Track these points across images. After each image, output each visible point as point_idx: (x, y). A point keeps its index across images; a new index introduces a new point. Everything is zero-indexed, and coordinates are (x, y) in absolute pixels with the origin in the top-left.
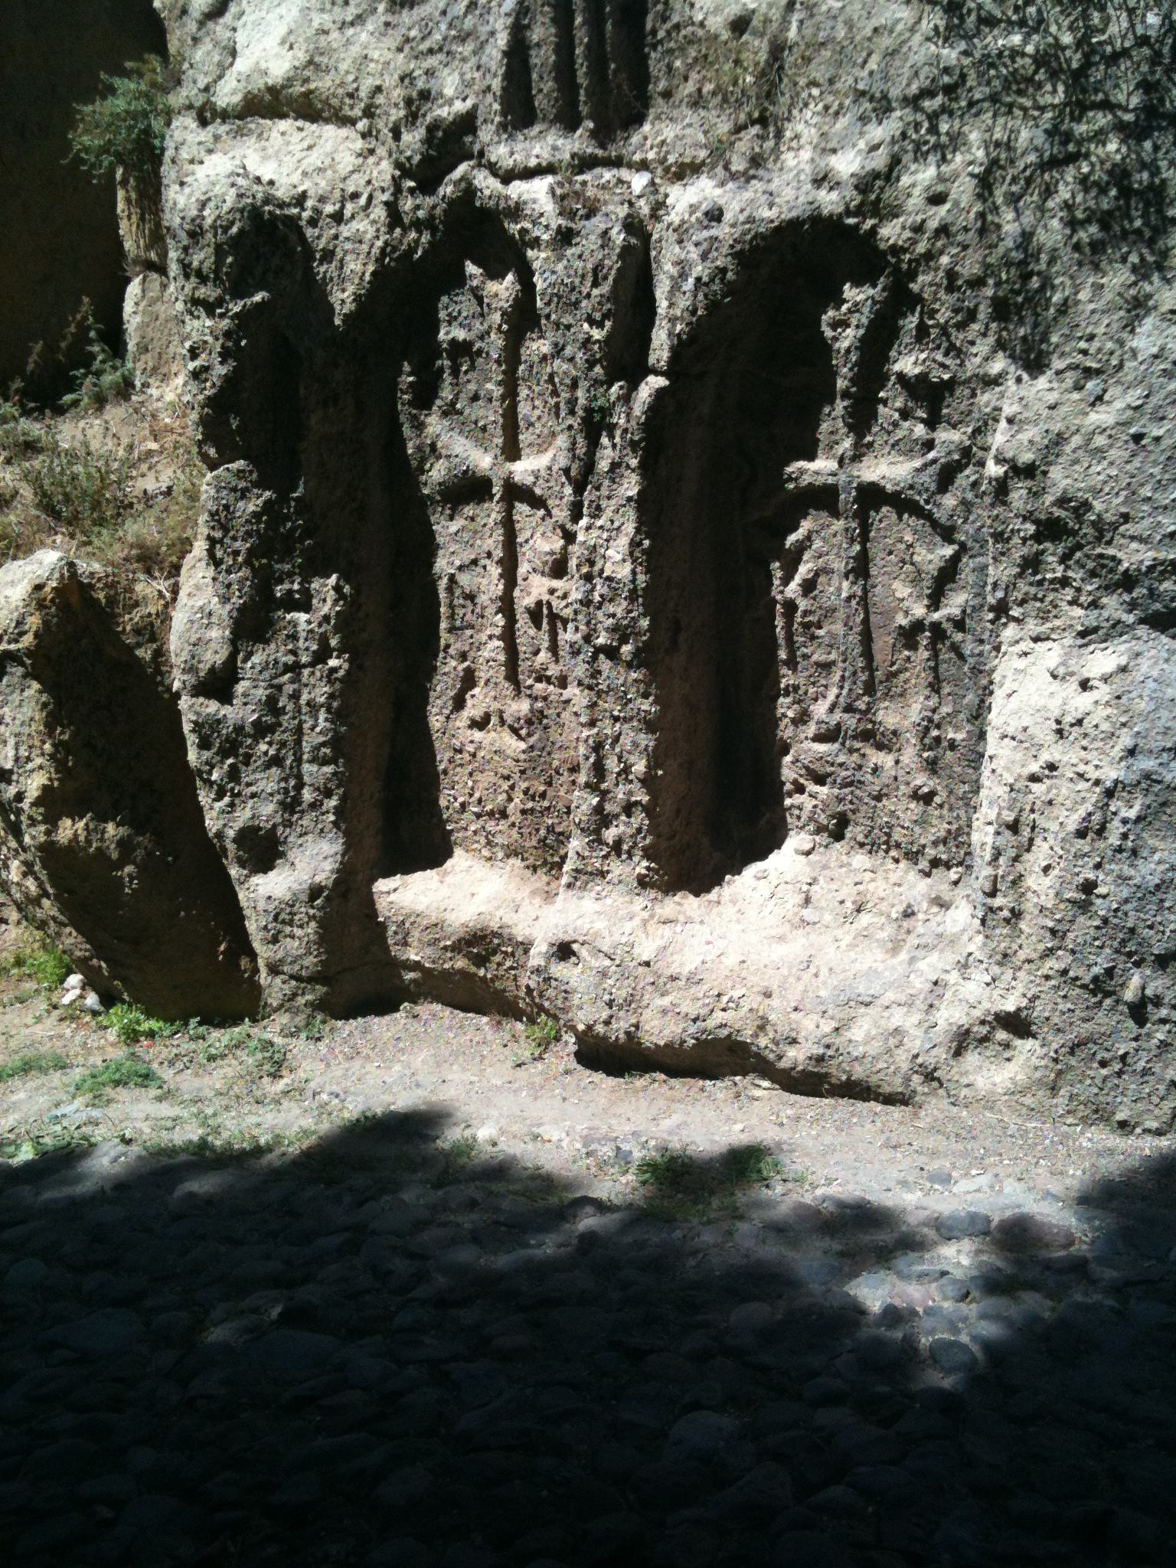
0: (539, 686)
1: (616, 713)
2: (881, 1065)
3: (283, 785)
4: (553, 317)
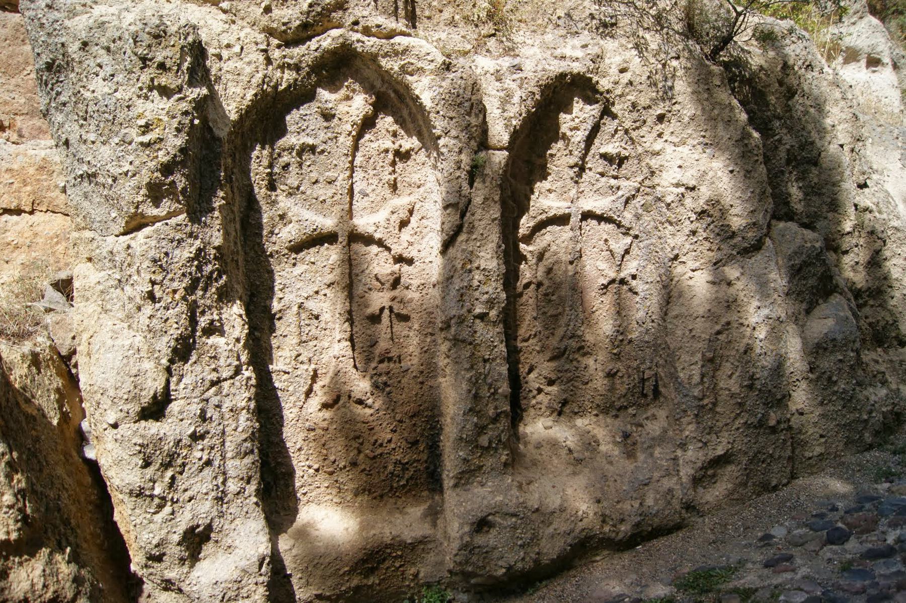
0: (381, 366)
1: (487, 357)
2: (666, 512)
4: (441, 113)
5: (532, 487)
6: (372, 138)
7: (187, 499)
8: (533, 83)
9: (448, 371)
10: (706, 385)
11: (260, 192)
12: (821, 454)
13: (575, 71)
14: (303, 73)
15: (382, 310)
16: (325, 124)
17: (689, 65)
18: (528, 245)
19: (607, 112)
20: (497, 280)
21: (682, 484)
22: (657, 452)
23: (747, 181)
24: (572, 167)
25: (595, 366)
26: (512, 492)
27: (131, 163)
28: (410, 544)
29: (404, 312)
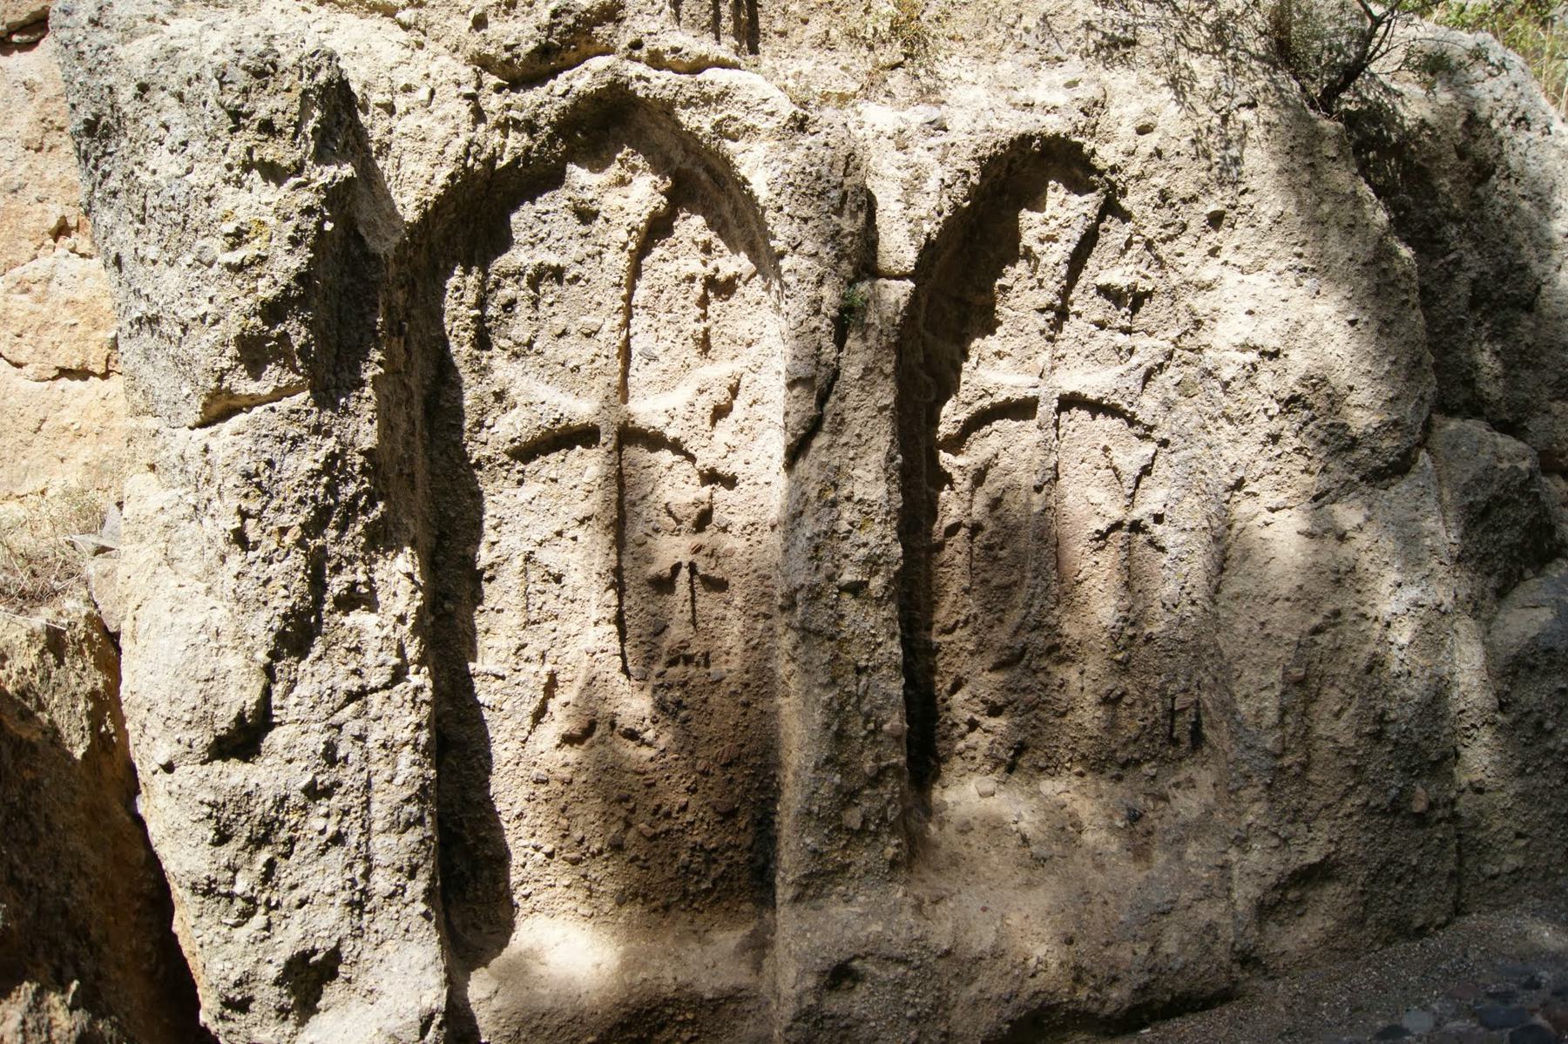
0: (672, 670)
1: (863, 663)
3: (348, 875)
4: (786, 210)
5: (941, 909)
6: (667, 255)
7: (295, 902)
8: (967, 153)
9: (793, 685)
10: (1290, 730)
11: (461, 351)
12: (1517, 870)
13: (1050, 131)
14: (541, 137)
15: (676, 568)
16: (583, 229)
17: (1274, 118)
18: (956, 455)
19: (1111, 208)
20: (886, 522)
21: (1234, 916)
22: (1192, 851)
23: (1384, 341)
24: (1042, 311)
25: (1082, 683)
26: (903, 917)
27: (211, 300)
28: (710, 1000)
29: (717, 574)
